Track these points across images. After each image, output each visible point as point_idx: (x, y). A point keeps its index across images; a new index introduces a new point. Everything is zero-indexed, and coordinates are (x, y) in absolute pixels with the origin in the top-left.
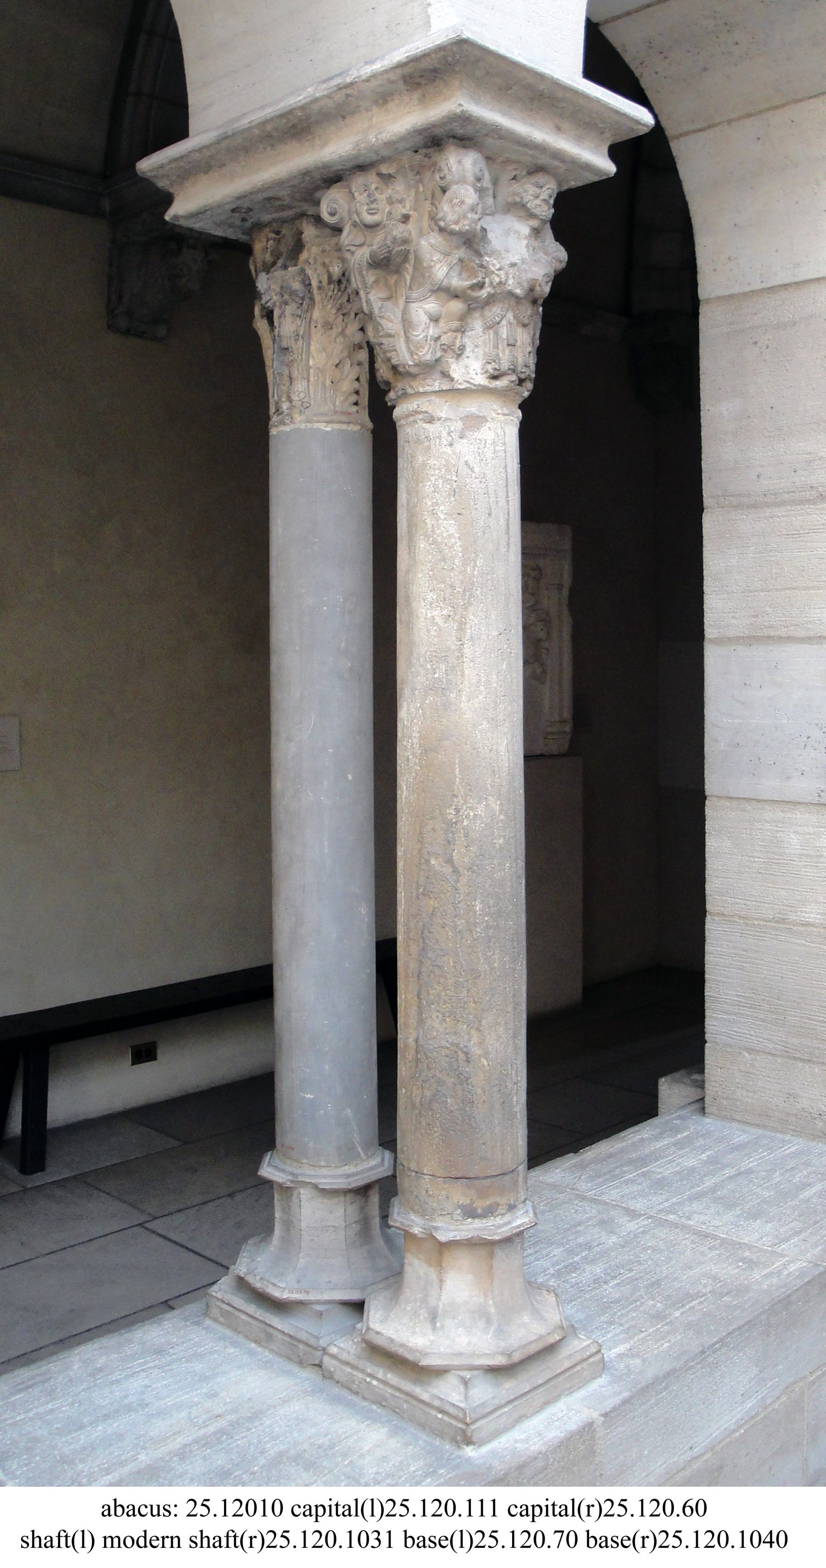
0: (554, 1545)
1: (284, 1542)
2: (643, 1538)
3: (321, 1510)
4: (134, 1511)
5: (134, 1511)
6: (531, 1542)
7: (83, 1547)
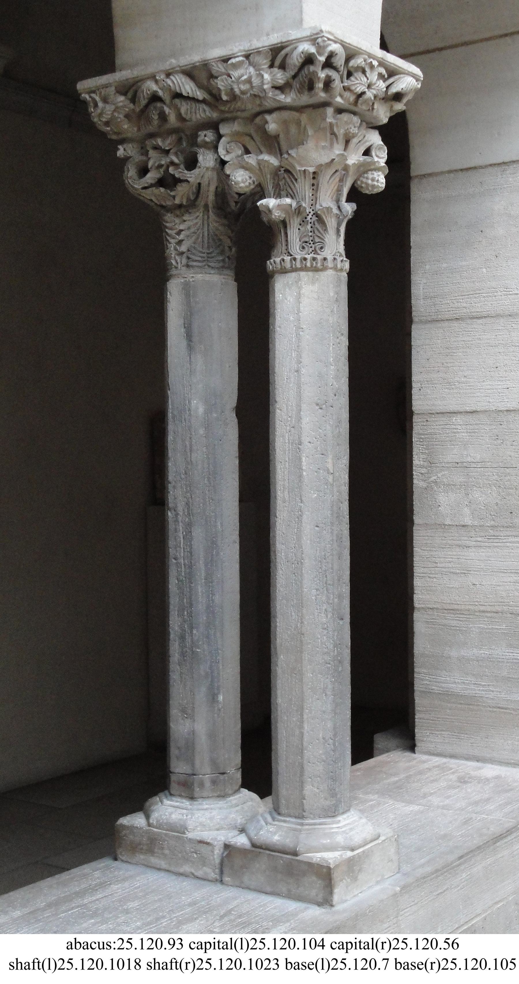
0: (382, 968)
1: (453, 966)
6: (367, 966)
7: (49, 969)
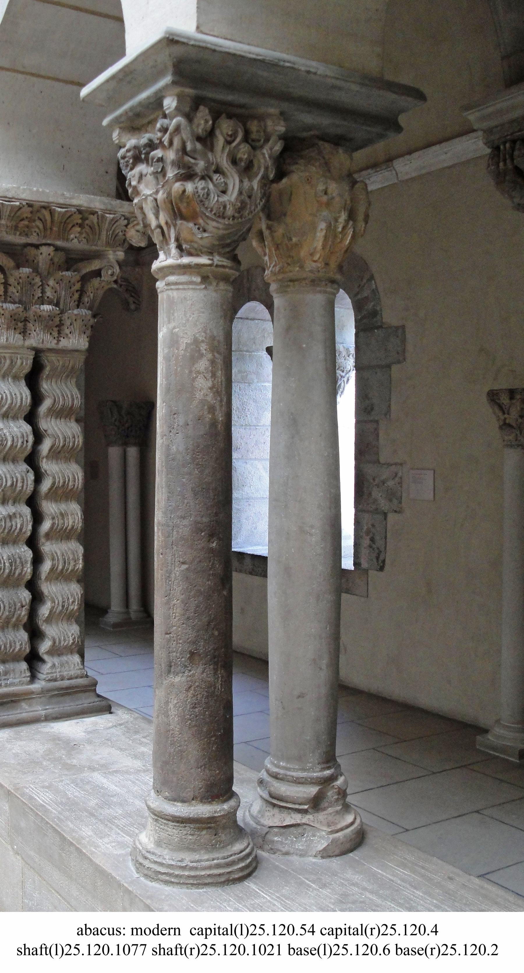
2: (191, 949)
3: (209, 931)
4: (97, 932)
5: (97, 932)
